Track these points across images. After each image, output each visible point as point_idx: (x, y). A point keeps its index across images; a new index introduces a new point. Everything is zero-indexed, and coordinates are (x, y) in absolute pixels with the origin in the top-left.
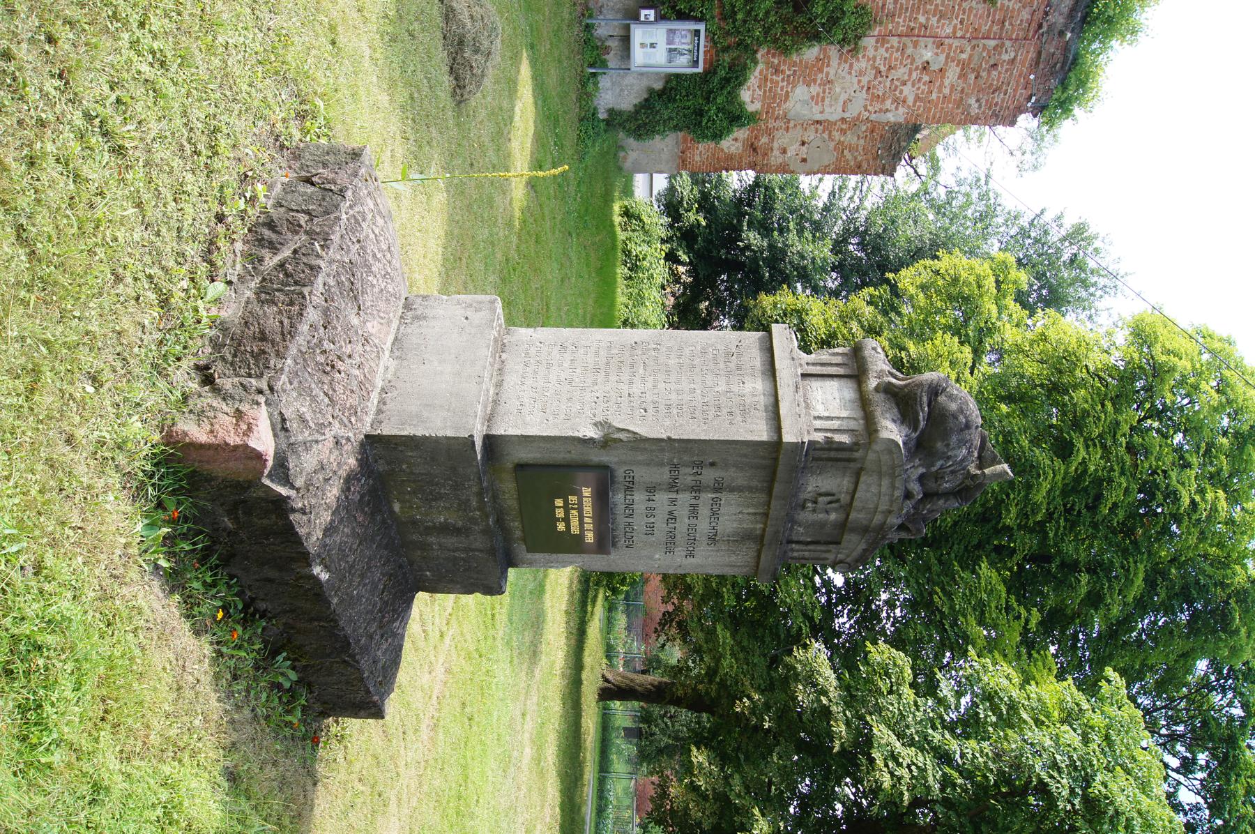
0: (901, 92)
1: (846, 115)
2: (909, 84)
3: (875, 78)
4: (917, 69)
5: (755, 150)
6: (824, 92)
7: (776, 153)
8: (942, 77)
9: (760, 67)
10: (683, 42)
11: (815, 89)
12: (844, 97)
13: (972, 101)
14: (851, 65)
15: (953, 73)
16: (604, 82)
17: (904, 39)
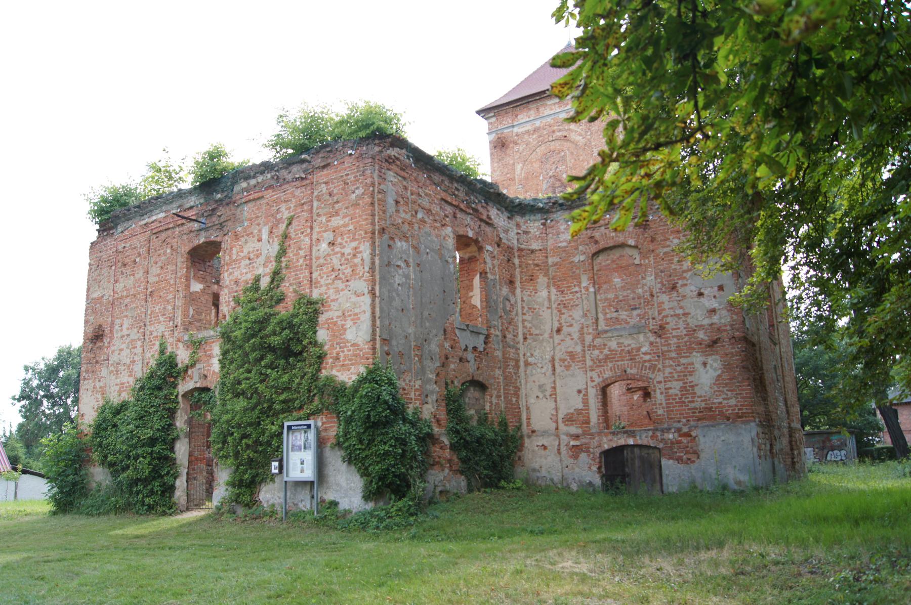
0: (349, 254)
1: (366, 291)
2: (343, 251)
3: (340, 279)
4: (333, 250)
5: (715, 342)
6: (350, 316)
7: (715, 319)
8: (338, 228)
9: (334, 372)
10: (298, 438)
11: (349, 323)
12: (354, 299)
13: (354, 196)
14: (332, 301)
15: (337, 221)
16: (344, 505)
17: (314, 268)
